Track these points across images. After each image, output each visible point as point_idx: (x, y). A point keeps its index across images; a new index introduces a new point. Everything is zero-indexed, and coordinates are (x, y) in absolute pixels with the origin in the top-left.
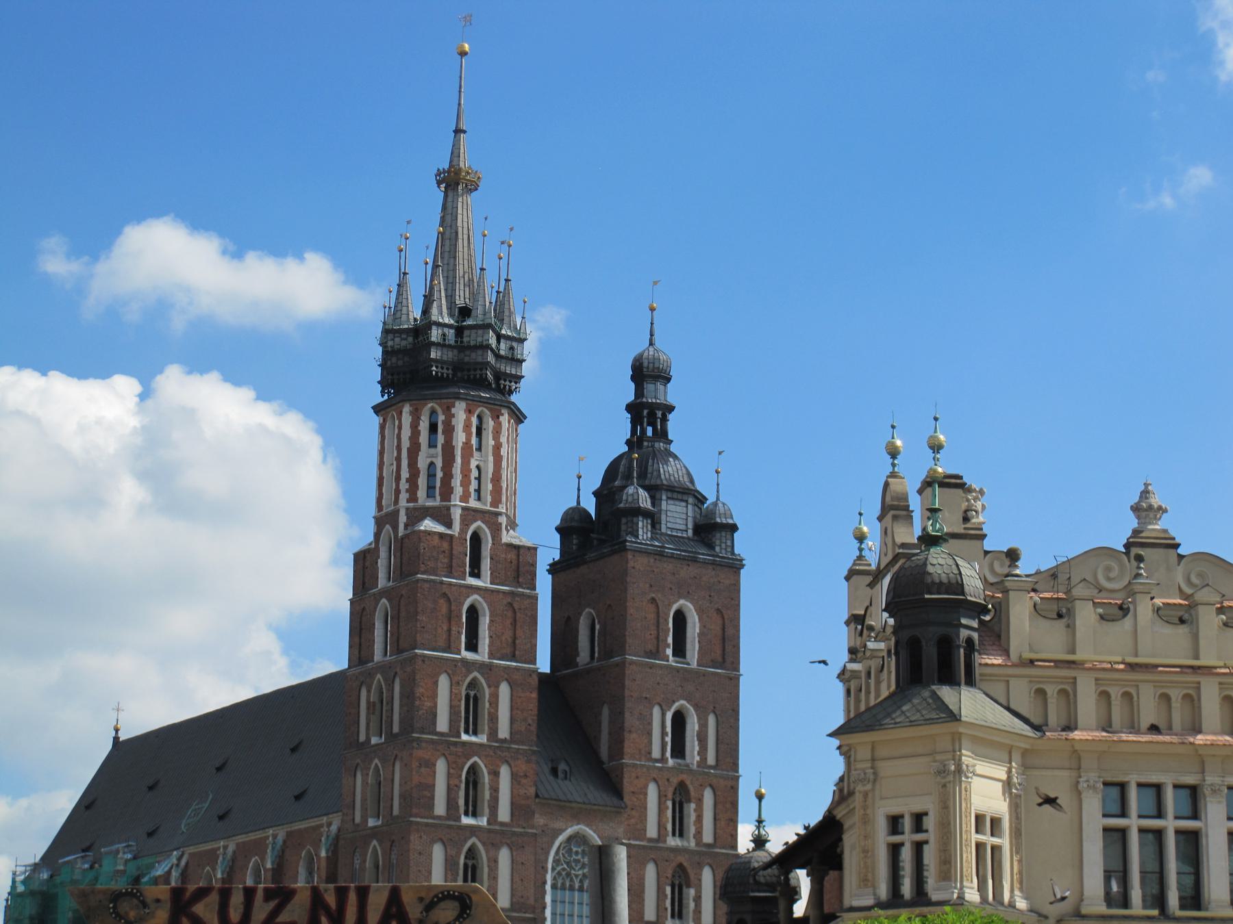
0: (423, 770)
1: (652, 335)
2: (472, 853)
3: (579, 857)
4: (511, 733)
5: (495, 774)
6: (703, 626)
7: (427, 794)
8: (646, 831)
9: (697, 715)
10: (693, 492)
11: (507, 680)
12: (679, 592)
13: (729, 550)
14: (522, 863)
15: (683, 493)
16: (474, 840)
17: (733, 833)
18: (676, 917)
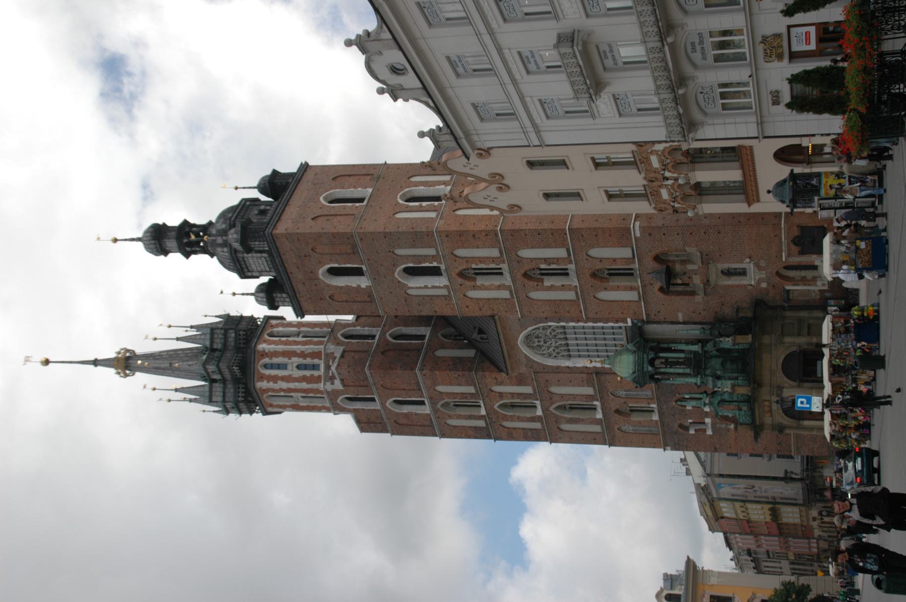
0: (514, 436)
1: (133, 240)
2: (562, 408)
3: (542, 340)
4: (469, 385)
5: (501, 395)
6: (331, 261)
7: (530, 433)
8: (505, 299)
9: (401, 265)
10: (234, 255)
11: (434, 389)
12: (315, 279)
13: (262, 243)
14: (558, 381)
15: (239, 261)
16: (551, 409)
17: (484, 234)
18: (567, 271)
